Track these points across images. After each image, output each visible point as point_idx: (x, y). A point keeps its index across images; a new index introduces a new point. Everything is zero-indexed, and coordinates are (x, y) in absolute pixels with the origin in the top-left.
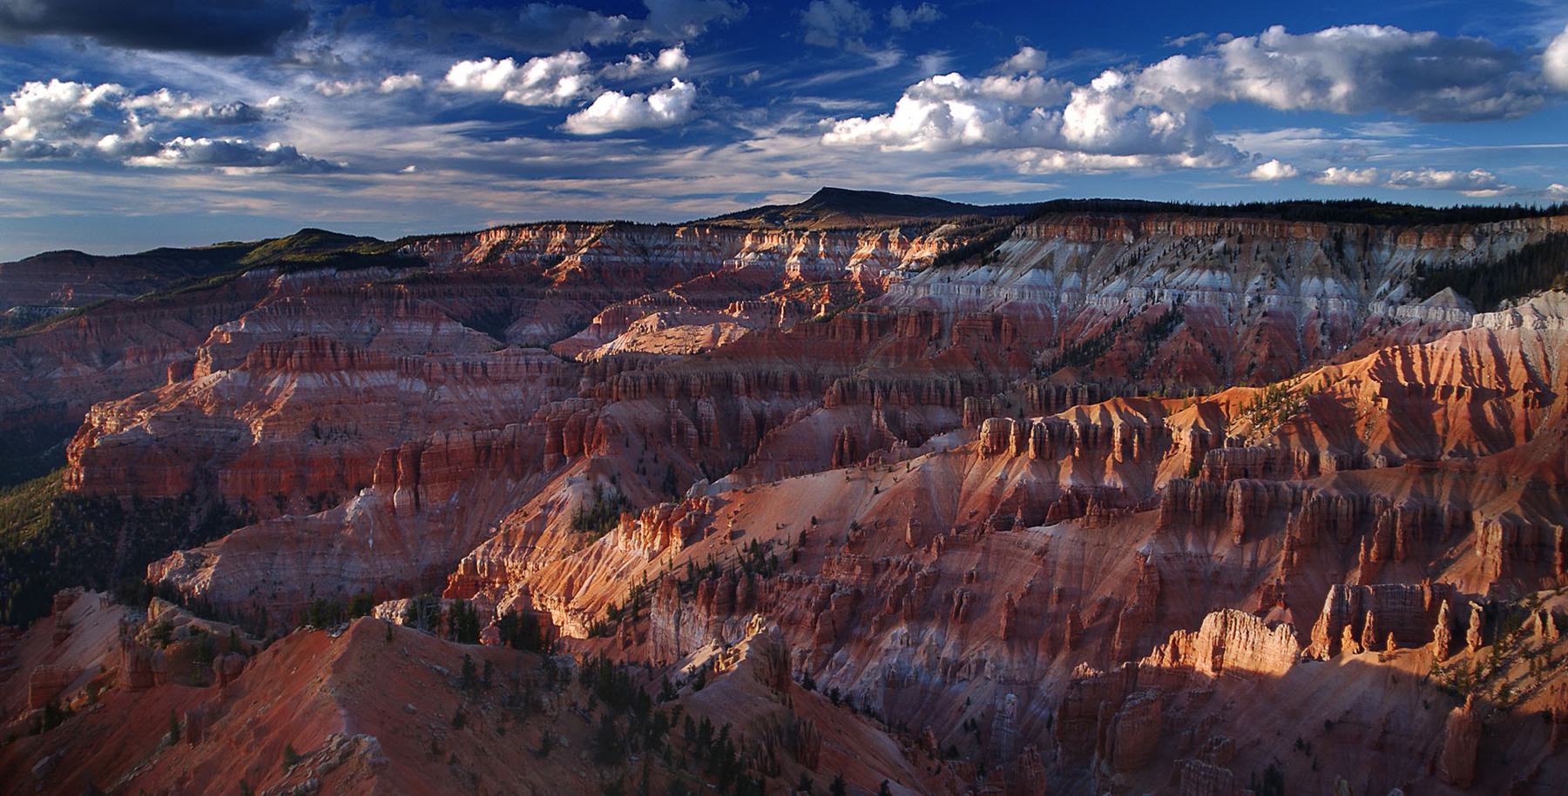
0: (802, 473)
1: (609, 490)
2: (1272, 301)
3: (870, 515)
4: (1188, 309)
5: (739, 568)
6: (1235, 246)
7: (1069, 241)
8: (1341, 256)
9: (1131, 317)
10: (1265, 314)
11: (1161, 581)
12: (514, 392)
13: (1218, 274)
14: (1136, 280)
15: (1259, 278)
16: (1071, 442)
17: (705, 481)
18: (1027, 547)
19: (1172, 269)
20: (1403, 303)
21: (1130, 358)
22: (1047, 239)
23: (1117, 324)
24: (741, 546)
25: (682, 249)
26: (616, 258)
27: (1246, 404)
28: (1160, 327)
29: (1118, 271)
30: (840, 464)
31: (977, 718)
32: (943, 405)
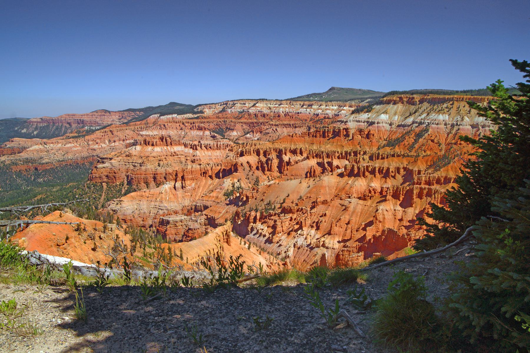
0: (288, 180)
3: (307, 194)
19: (428, 114)
25: (283, 107)
29: (410, 115)
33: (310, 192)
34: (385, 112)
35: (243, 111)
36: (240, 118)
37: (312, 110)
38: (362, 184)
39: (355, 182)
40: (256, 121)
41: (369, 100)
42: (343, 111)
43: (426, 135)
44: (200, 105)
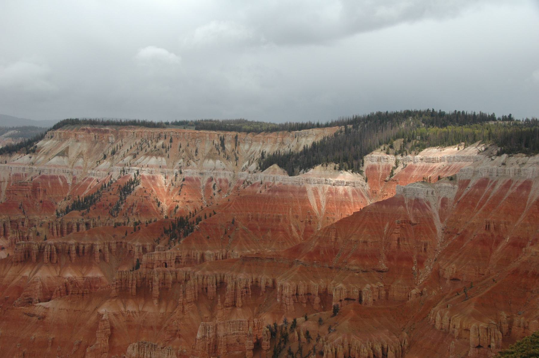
2: (189, 173)
4: (143, 177)
6: (168, 144)
7: (78, 141)
8: (224, 148)
9: (112, 183)
10: (184, 180)
11: (112, 328)
13: (160, 158)
14: (115, 162)
15: (181, 160)
16: (69, 253)
19: (135, 156)
20: (255, 172)
21: (110, 205)
23: (103, 187)
27: (168, 228)
29: (105, 157)
34: (64, 153)
38: (50, 275)
39: (36, 272)
41: (12, 132)
43: (137, 188)
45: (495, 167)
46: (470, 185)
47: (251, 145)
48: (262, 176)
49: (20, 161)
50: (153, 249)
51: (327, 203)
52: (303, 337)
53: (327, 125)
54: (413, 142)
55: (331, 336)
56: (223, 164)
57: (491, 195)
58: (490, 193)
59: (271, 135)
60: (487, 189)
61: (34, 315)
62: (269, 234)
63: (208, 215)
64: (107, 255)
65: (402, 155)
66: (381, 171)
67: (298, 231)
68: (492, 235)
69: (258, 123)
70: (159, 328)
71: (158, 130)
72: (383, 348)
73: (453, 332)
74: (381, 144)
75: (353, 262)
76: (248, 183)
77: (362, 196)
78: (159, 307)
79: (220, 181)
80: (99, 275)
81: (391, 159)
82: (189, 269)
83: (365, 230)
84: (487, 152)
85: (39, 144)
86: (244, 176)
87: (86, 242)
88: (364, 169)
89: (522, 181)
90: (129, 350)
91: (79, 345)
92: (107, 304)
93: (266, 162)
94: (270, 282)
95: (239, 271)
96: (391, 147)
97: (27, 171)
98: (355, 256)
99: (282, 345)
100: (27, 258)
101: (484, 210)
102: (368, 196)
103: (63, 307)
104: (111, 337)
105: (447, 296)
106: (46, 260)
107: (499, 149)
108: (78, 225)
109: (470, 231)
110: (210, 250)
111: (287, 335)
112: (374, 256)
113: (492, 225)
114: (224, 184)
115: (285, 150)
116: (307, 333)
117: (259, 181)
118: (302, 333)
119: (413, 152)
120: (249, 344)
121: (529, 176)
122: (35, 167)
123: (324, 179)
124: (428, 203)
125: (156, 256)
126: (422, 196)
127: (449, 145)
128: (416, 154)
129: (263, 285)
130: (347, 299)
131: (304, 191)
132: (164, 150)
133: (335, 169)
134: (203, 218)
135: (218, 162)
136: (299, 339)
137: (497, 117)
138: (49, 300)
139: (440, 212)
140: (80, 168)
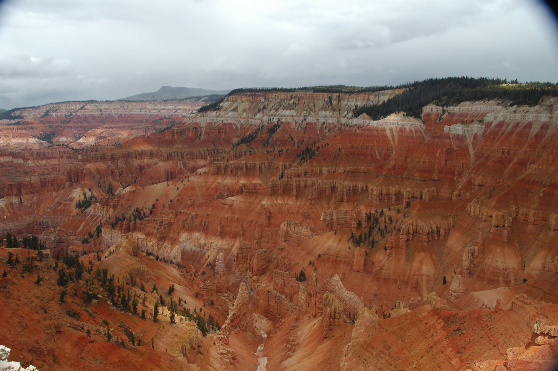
0: (153, 184)
1: (89, 194)
2: (310, 119)
3: (176, 197)
4: (282, 123)
5: (132, 218)
6: (297, 102)
7: (243, 102)
8: (331, 104)
10: (307, 124)
12: (55, 162)
13: (292, 111)
15: (305, 112)
16: (242, 169)
17: (122, 189)
18: (226, 204)
19: (277, 110)
22: (236, 101)
23: (259, 129)
24: (133, 210)
25: (114, 109)
26: (90, 113)
27: (299, 154)
28: (273, 129)
29: (259, 111)
30: (168, 180)
31: (211, 262)
32: (202, 158)
33: (179, 195)
34: (235, 110)
35: (71, 114)
36: (68, 122)
37: (147, 110)
40: (86, 124)
41: (203, 99)
42: (179, 111)
43: (278, 130)
44: (17, 109)
45: (509, 113)
46: (492, 126)
47: (348, 101)
48: (355, 121)
49: (211, 115)
50: (290, 166)
51: (399, 137)
52: (387, 220)
53: (397, 88)
54: (455, 97)
55: (406, 219)
56: (331, 114)
57: (506, 132)
58: (505, 130)
59: (361, 95)
60: (504, 128)
61: (226, 204)
62: (362, 157)
63: (324, 145)
64: (263, 170)
65: (447, 107)
66: (433, 117)
67: (380, 155)
68: (506, 158)
69: (351, 87)
70: (297, 213)
71: (290, 94)
72: (437, 227)
73: (482, 218)
74: (433, 100)
75: (417, 175)
76: (347, 125)
77: (421, 133)
78: (297, 201)
79: (329, 124)
80: (259, 182)
81: (440, 109)
82: (314, 179)
83: (424, 155)
84: (503, 104)
85: (221, 104)
86: (344, 121)
87: (251, 162)
88: (422, 115)
89: (526, 123)
90: (282, 225)
91: (252, 222)
92: (266, 198)
93: (358, 112)
94: (365, 188)
95: (345, 180)
96: (440, 101)
97: (215, 121)
98: (418, 171)
99: (375, 225)
100: (218, 172)
101: (501, 142)
102: (425, 133)
103: (241, 200)
104: (269, 218)
105: (478, 196)
106: (229, 173)
107: (512, 102)
108: (245, 152)
109: (492, 155)
110: (326, 167)
111: (378, 219)
112: (430, 171)
113: (506, 151)
114: (331, 126)
115: (370, 104)
116: (390, 219)
117: (355, 123)
118: (387, 218)
119: (454, 104)
120: (354, 224)
121: (530, 120)
122: (219, 119)
123: (396, 122)
124: (465, 137)
125: (292, 170)
126: (461, 133)
127: (479, 99)
128: (456, 106)
129: (359, 188)
130: (413, 198)
131: (384, 130)
132: (294, 106)
133: (404, 115)
134: (321, 148)
135: (328, 112)
136: (385, 221)
137: (507, 81)
138: (233, 196)
139: (473, 143)
140: (244, 118)
